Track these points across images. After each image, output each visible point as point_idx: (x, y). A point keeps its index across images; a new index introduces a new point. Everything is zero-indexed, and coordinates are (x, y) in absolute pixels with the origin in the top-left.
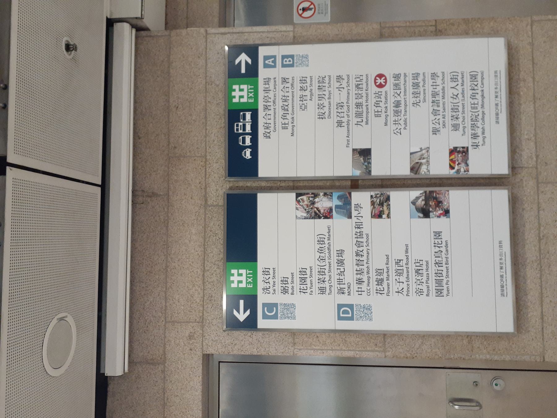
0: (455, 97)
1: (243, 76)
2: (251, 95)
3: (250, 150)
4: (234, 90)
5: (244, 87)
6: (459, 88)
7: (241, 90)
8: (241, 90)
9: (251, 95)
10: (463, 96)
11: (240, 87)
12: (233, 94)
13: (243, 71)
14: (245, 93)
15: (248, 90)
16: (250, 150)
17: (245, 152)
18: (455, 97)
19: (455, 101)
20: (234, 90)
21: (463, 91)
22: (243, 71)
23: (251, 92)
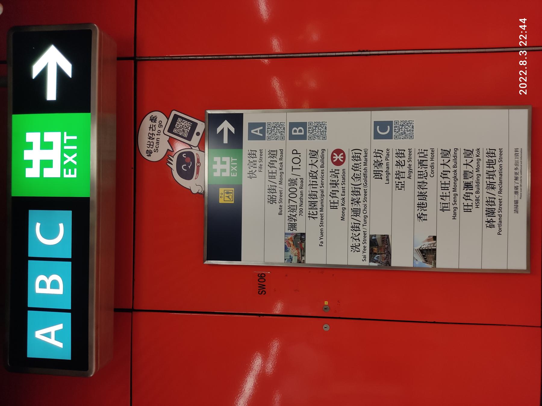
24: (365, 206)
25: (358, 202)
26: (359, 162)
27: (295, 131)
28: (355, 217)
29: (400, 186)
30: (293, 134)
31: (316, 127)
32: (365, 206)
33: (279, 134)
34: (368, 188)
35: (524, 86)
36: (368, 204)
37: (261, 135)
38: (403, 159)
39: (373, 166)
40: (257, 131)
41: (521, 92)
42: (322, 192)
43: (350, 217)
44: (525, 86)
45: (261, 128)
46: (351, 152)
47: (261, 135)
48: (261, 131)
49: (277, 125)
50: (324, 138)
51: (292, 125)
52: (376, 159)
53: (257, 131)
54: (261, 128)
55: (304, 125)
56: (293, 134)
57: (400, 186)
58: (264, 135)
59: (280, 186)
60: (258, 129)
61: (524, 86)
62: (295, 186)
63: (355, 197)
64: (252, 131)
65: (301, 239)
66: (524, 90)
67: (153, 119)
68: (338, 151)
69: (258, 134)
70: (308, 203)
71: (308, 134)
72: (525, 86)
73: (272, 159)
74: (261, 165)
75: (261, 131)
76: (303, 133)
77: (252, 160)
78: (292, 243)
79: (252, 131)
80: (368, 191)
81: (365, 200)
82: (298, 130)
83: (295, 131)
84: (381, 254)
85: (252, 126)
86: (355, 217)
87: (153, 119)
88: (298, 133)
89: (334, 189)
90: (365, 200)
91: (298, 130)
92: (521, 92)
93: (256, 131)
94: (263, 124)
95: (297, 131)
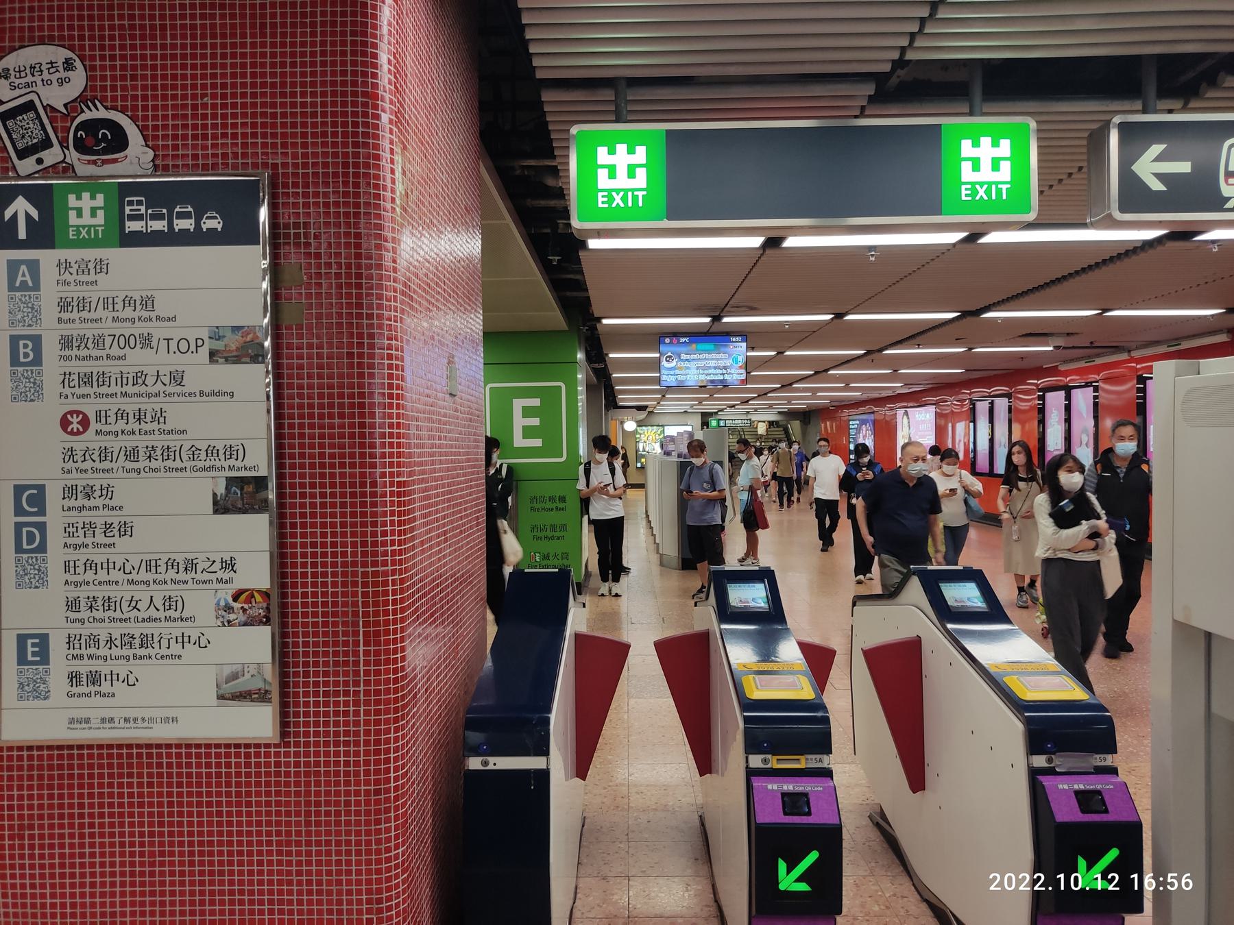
0: (133, 604)
2: (84, 233)
5: (100, 218)
6: (152, 611)
7: (93, 212)
8: (93, 212)
9: (84, 233)
10: (144, 620)
11: (100, 208)
14: (87, 220)
18: (133, 604)
21: (155, 620)
23: (88, 233)
24: (158, 470)
25: (150, 457)
26: (222, 456)
27: (26, 346)
28: (123, 453)
29: (71, 530)
30: (21, 343)
31: (34, 383)
32: (158, 470)
33: (19, 317)
34: (188, 474)
35: (1010, 885)
36: (162, 474)
37: (18, 284)
38: (117, 534)
39: (84, 483)
40: (24, 275)
42: (156, 395)
43: (123, 444)
44: (1010, 885)
45: (30, 284)
46: (239, 442)
47: (18, 284)
48: (24, 283)
49: (36, 313)
50: (14, 399)
51: (37, 340)
52: (97, 488)
53: (24, 275)
54: (30, 284)
55: (38, 361)
56: (21, 343)
57: (71, 530)
58: (18, 289)
59: (110, 319)
60: (28, 278)
61: (1010, 885)
62: (139, 346)
63: (159, 452)
64: (23, 268)
65: (257, 356)
66: (1001, 884)
67: (68, 65)
68: (65, 423)
69: (20, 278)
70: (88, 370)
71: (20, 369)
72: (1010, 885)
73: (138, 303)
74: (69, 284)
75: (24, 283)
76: (22, 359)
77: (91, 266)
78: (249, 339)
79: (23, 268)
80: (184, 474)
81: (170, 469)
82: (28, 350)
83: (26, 346)
84: (242, 499)
85: (34, 266)
86: (123, 453)
87: (68, 65)
88: (22, 350)
89: (131, 416)
90: (170, 469)
91: (28, 350)
93: (24, 275)
94: (37, 287)
95: (26, 349)
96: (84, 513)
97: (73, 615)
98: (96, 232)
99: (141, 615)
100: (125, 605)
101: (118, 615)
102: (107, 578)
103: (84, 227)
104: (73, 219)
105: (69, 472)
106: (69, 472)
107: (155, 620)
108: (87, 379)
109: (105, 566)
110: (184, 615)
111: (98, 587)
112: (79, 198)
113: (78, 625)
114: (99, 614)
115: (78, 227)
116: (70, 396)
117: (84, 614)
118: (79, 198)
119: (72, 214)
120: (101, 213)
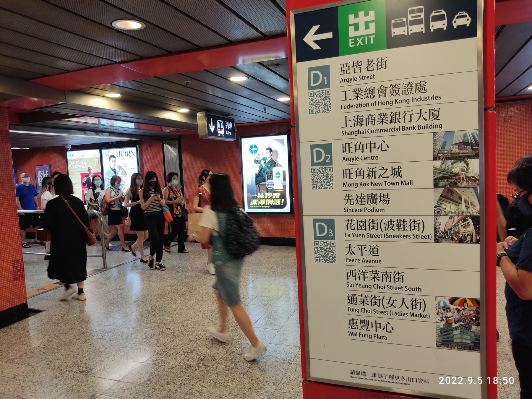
0: (391, 302)
1: (336, 35)
2: (360, 41)
3: (468, 23)
4: (367, 14)
7: (367, 26)
8: (367, 26)
9: (360, 41)
10: (396, 314)
12: (361, 14)
13: (329, 35)
14: (362, 31)
15: (368, 35)
16: (468, 23)
17: (465, 16)
18: (391, 302)
19: (386, 302)
20: (367, 14)
21: (404, 314)
22: (329, 35)
23: (363, 41)
41: (441, 379)
85: (325, 70)
92: (441, 379)
96: (359, 135)
97: (353, 307)
98: (369, 39)
99: (395, 310)
100: (386, 302)
101: (381, 309)
102: (370, 155)
103: (359, 37)
104: (352, 33)
105: (352, 285)
106: (352, 285)
107: (404, 314)
108: (362, 225)
109: (369, 146)
110: (423, 314)
111: (364, 162)
112: (356, 16)
113: (355, 313)
114: (368, 307)
115: (355, 38)
116: (351, 235)
117: (359, 306)
118: (356, 16)
119: (351, 29)
120: (372, 26)
